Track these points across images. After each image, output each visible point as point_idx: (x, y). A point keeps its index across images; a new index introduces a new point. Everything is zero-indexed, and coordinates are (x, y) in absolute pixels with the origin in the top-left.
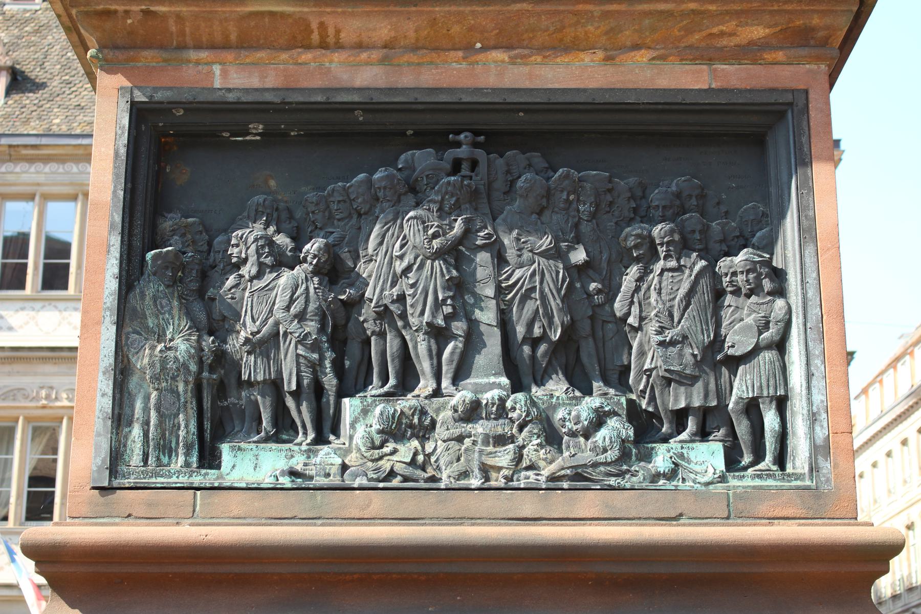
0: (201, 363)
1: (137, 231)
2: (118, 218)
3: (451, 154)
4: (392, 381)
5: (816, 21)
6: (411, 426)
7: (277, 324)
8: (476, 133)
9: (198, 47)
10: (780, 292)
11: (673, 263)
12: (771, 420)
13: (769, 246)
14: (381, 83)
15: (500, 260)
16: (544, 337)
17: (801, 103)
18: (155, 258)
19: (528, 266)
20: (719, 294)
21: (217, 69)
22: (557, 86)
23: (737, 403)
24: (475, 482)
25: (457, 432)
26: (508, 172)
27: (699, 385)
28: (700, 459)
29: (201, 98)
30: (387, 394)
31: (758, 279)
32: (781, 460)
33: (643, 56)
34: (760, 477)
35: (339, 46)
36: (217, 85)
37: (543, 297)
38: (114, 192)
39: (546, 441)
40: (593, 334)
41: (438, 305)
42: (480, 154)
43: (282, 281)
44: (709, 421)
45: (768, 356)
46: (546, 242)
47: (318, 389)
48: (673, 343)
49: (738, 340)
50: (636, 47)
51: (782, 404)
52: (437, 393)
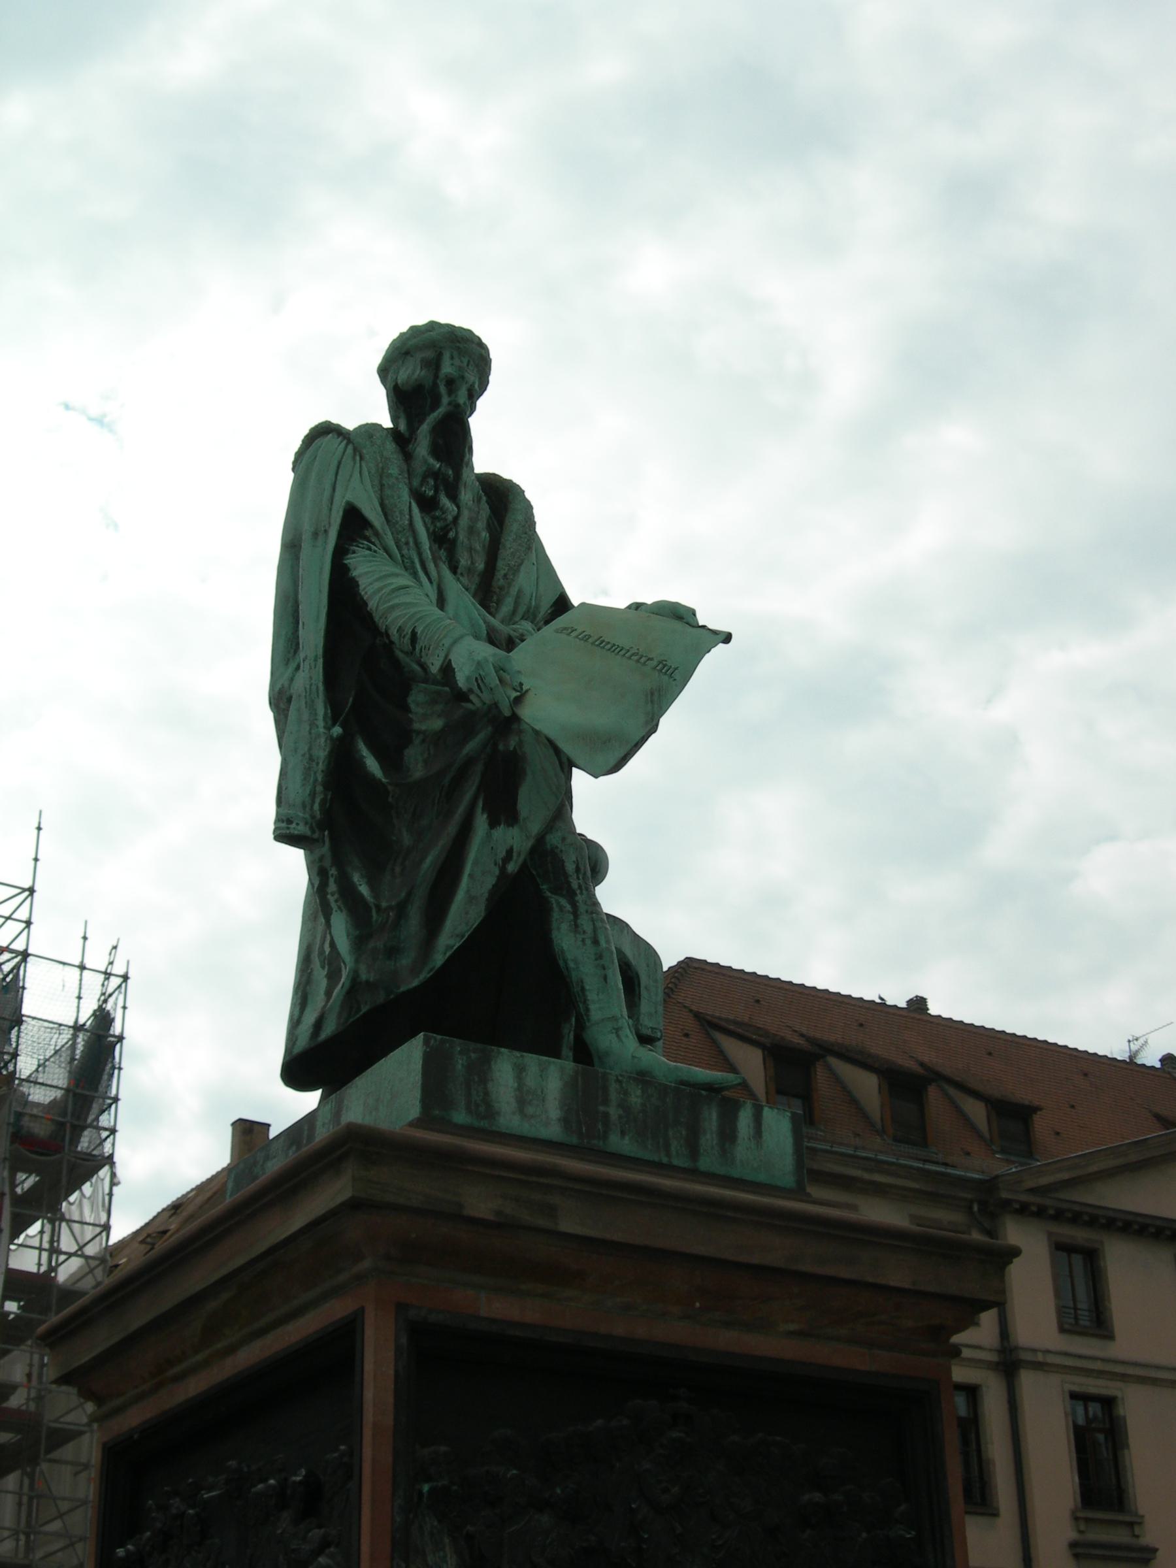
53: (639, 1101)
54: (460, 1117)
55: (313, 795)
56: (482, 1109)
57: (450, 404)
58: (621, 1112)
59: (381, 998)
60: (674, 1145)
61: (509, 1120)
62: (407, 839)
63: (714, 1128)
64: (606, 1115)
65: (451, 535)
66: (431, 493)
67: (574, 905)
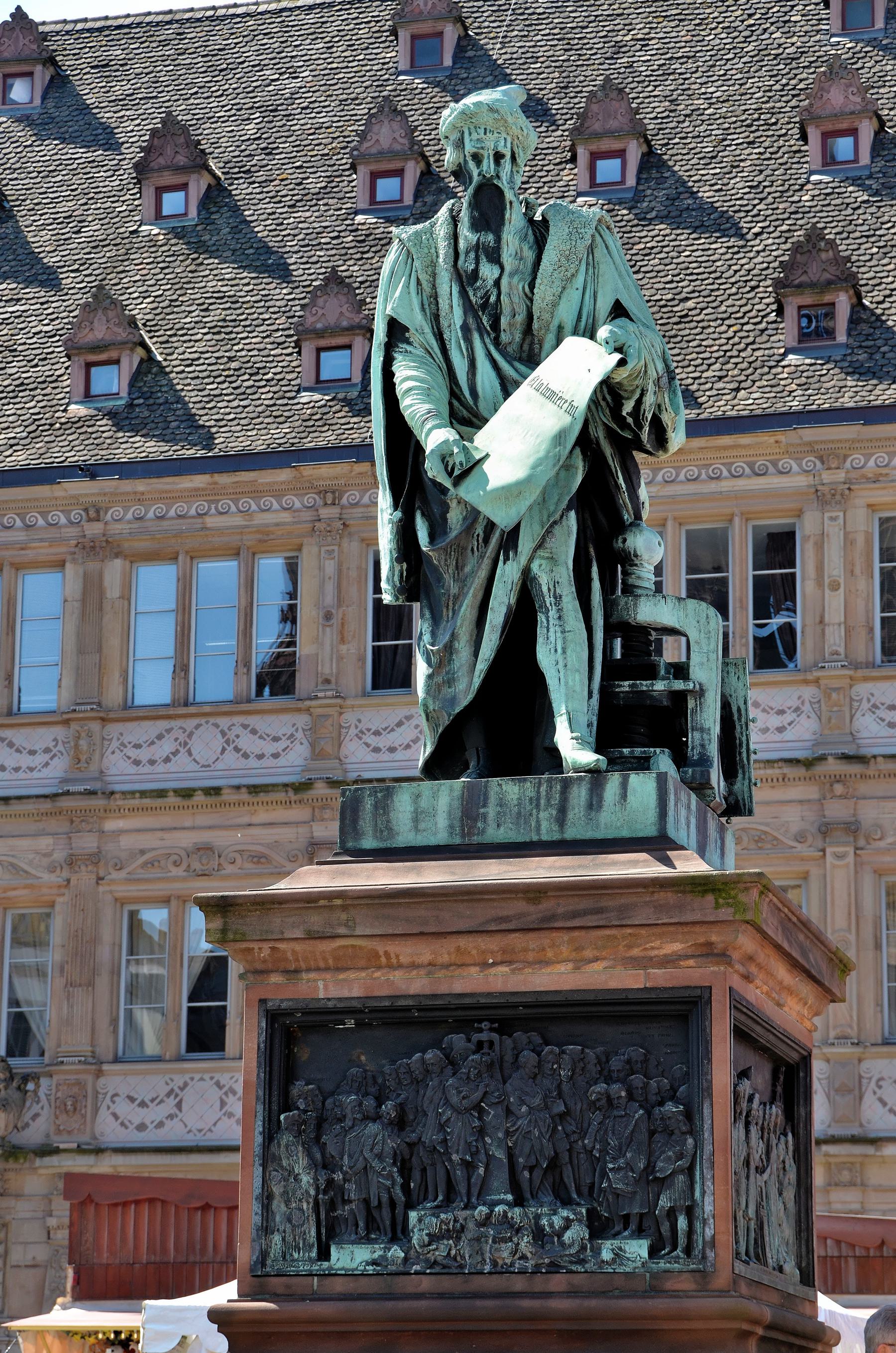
0: (317, 1189)
1: (275, 1099)
2: (261, 1093)
3: (476, 1037)
4: (440, 1198)
5: (714, 938)
6: (448, 1230)
8: (492, 1021)
9: (309, 970)
12: (682, 1223)
14: (428, 991)
17: (706, 996)
18: (285, 1118)
21: (321, 984)
22: (542, 989)
23: (660, 1210)
24: (487, 1268)
26: (514, 1048)
28: (632, 1250)
29: (311, 1006)
30: (437, 1207)
32: (688, 1251)
33: (598, 966)
34: (670, 1263)
35: (400, 966)
36: (321, 996)
38: (258, 1075)
39: (533, 1238)
40: (571, 1162)
42: (495, 1036)
47: (393, 1204)
49: (664, 1168)
50: (596, 959)
53: (517, 796)
54: (369, 843)
55: (392, 569)
56: (385, 833)
57: (479, 175)
58: (499, 809)
59: (445, 721)
60: (544, 825)
61: (405, 837)
62: (454, 590)
63: (582, 803)
64: (485, 816)
65: (493, 299)
66: (472, 267)
67: (548, 621)
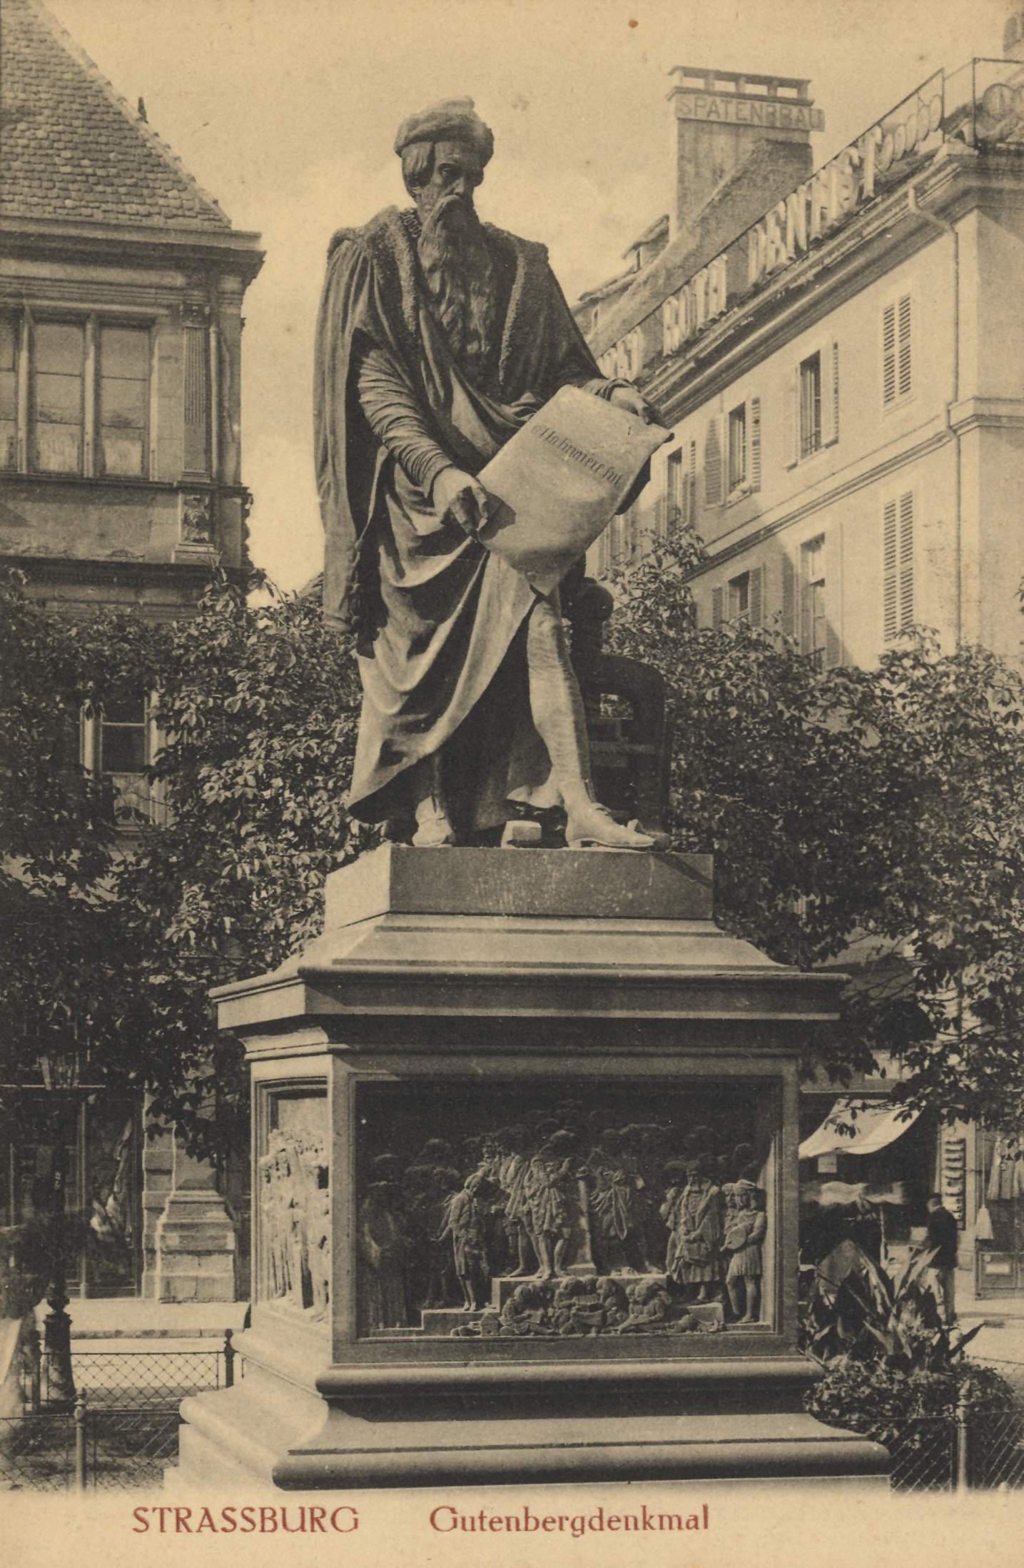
7: (451, 1231)
10: (762, 1207)
11: (696, 1188)
12: (750, 1288)
13: (754, 1175)
15: (591, 1185)
16: (616, 1236)
19: (610, 1193)
20: (723, 1206)
25: (566, 1302)
27: (708, 1268)
31: (748, 1200)
32: (756, 1317)
37: (618, 1213)
41: (552, 1219)
43: (453, 1201)
44: (714, 1289)
45: (750, 1250)
46: (618, 1175)
48: (695, 1241)
49: (732, 1239)
51: (757, 1279)
52: (553, 1275)
